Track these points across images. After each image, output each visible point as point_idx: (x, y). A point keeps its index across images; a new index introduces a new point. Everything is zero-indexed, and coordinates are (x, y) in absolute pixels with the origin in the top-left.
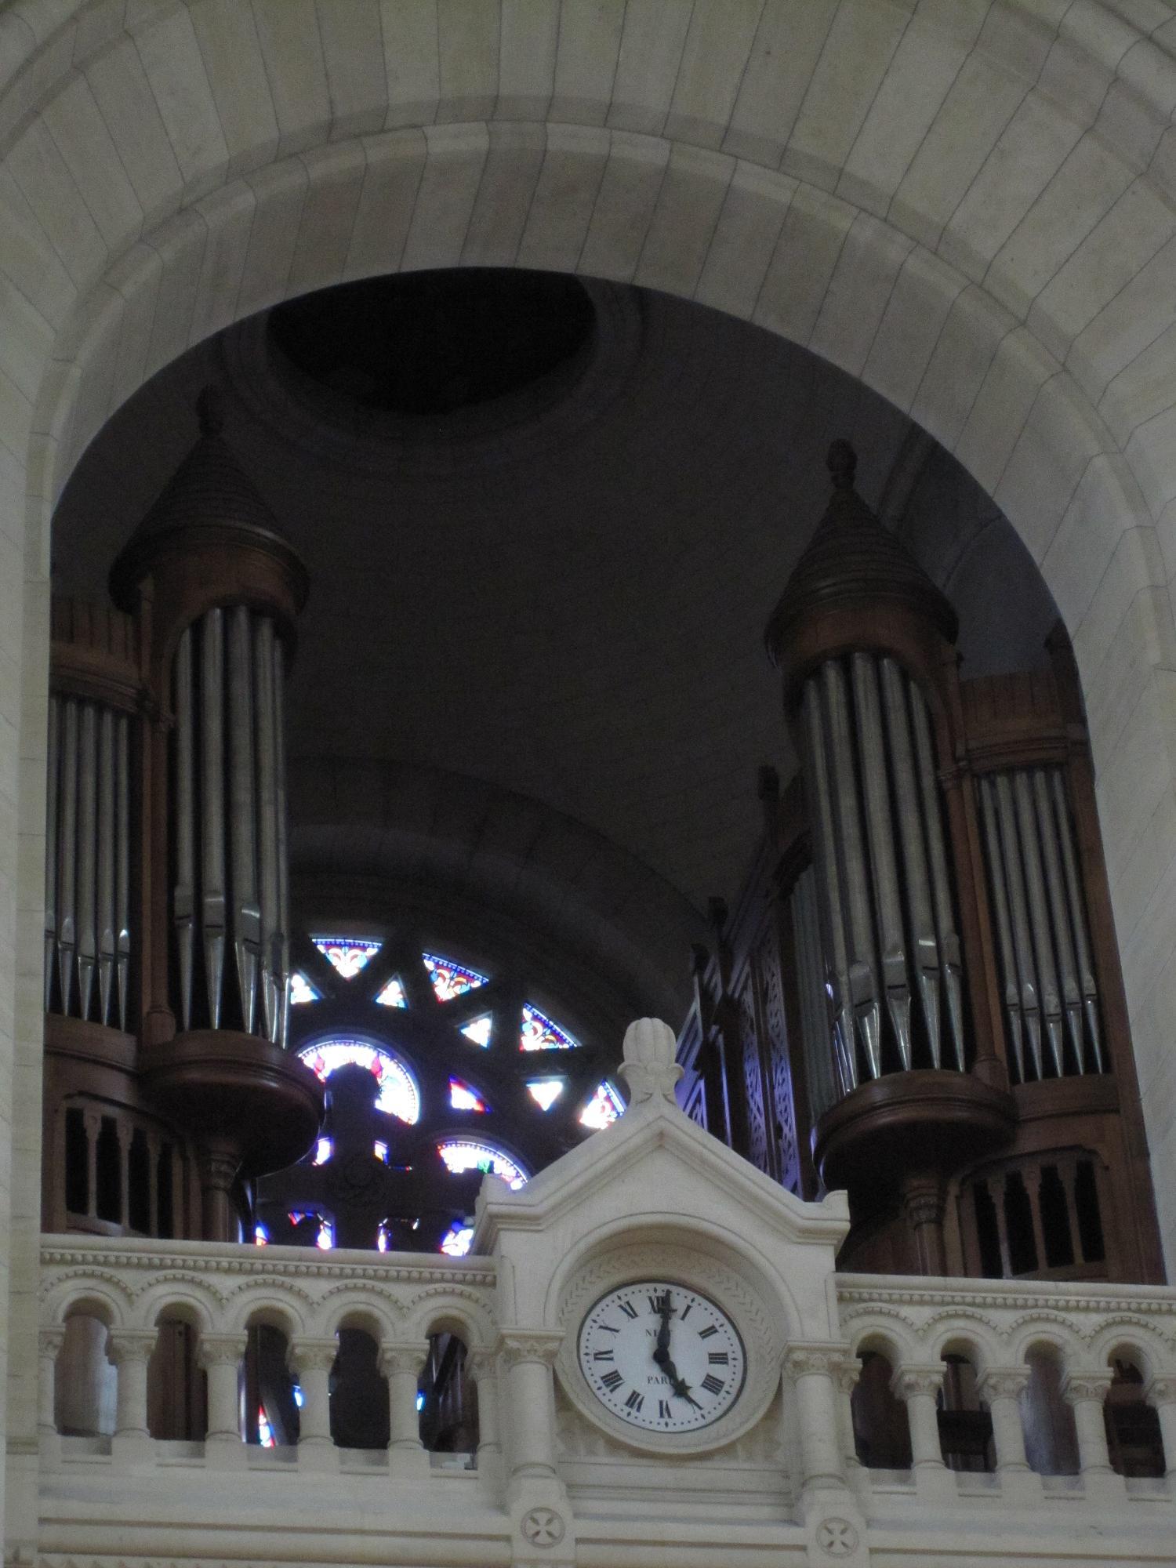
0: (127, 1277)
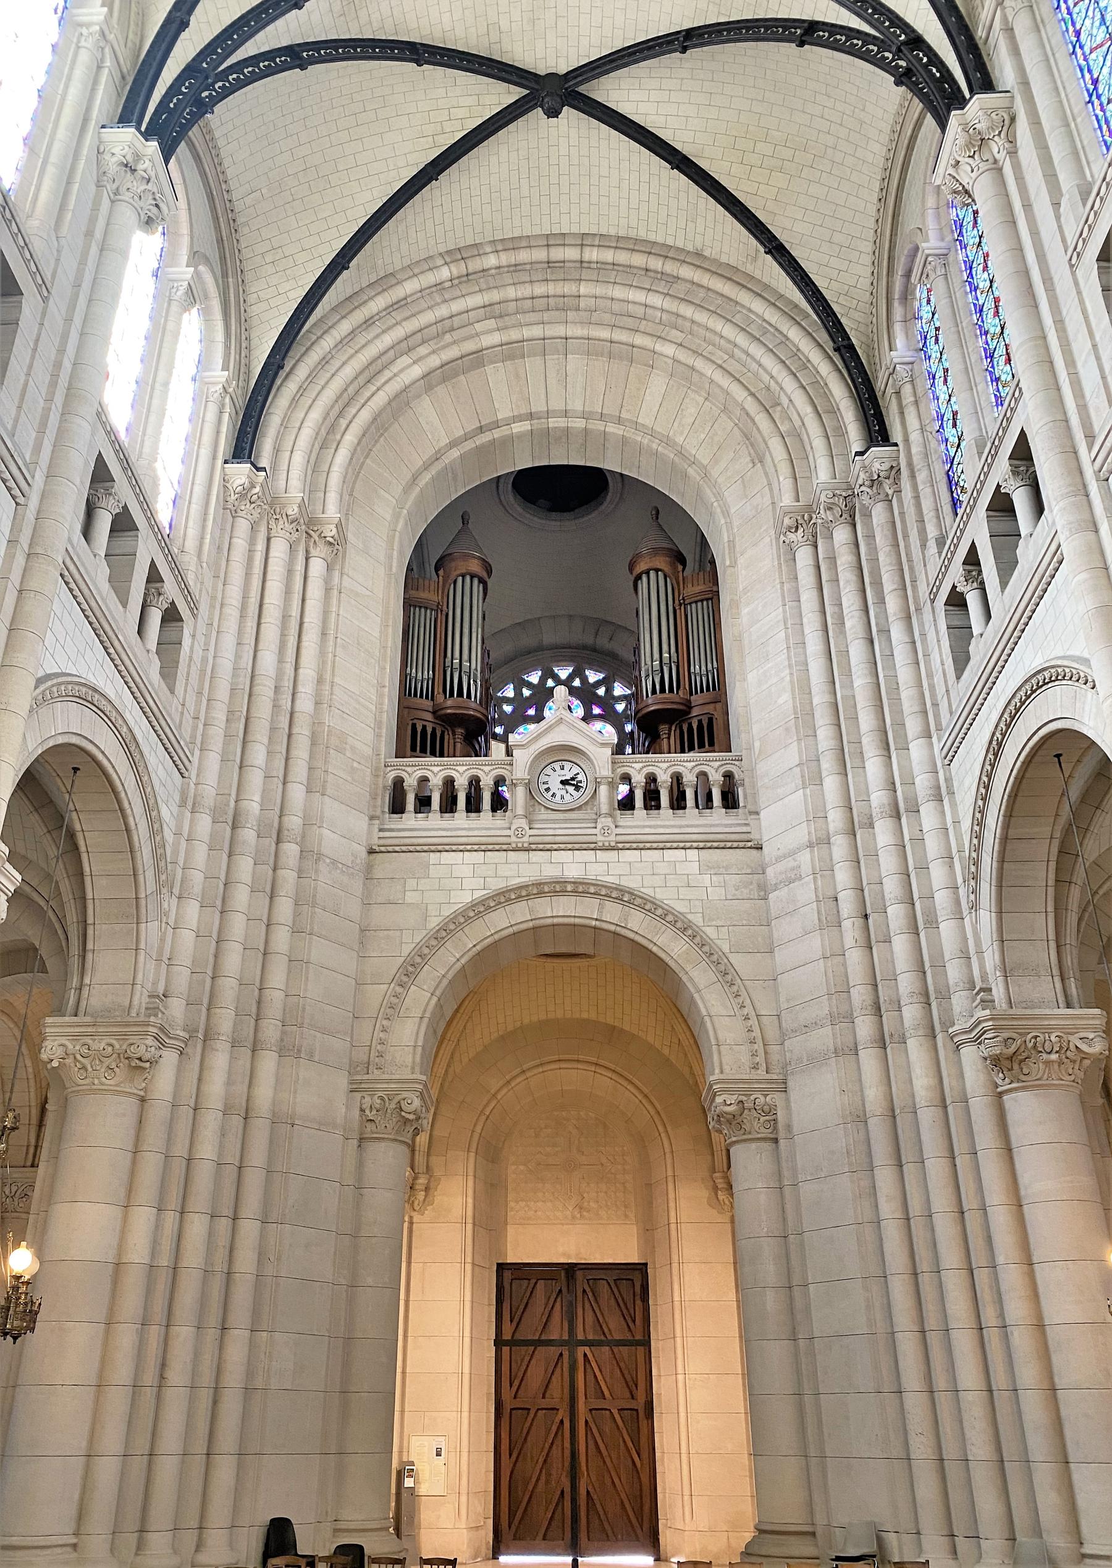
0: (409, 769)
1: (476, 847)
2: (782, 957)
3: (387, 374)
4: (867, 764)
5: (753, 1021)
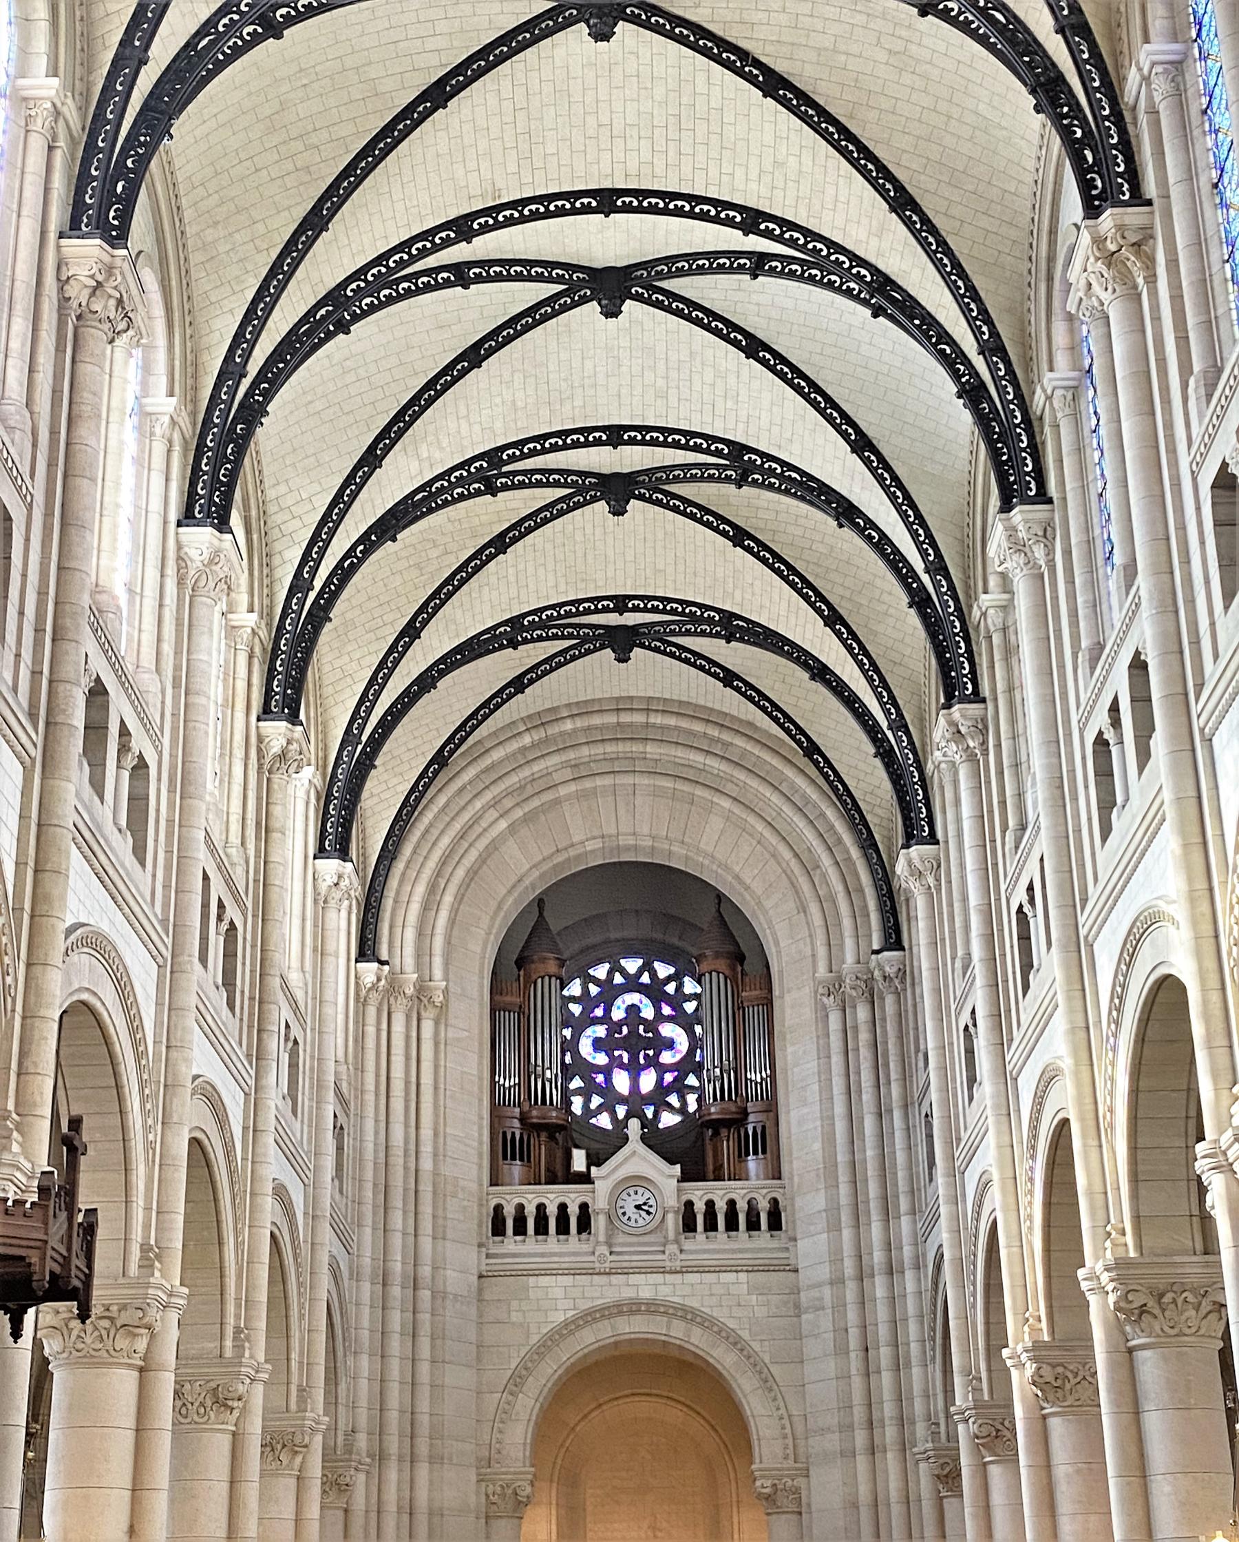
0: (507, 1197)
2: (808, 1368)
3: (478, 829)
4: (873, 1225)
5: (786, 1422)
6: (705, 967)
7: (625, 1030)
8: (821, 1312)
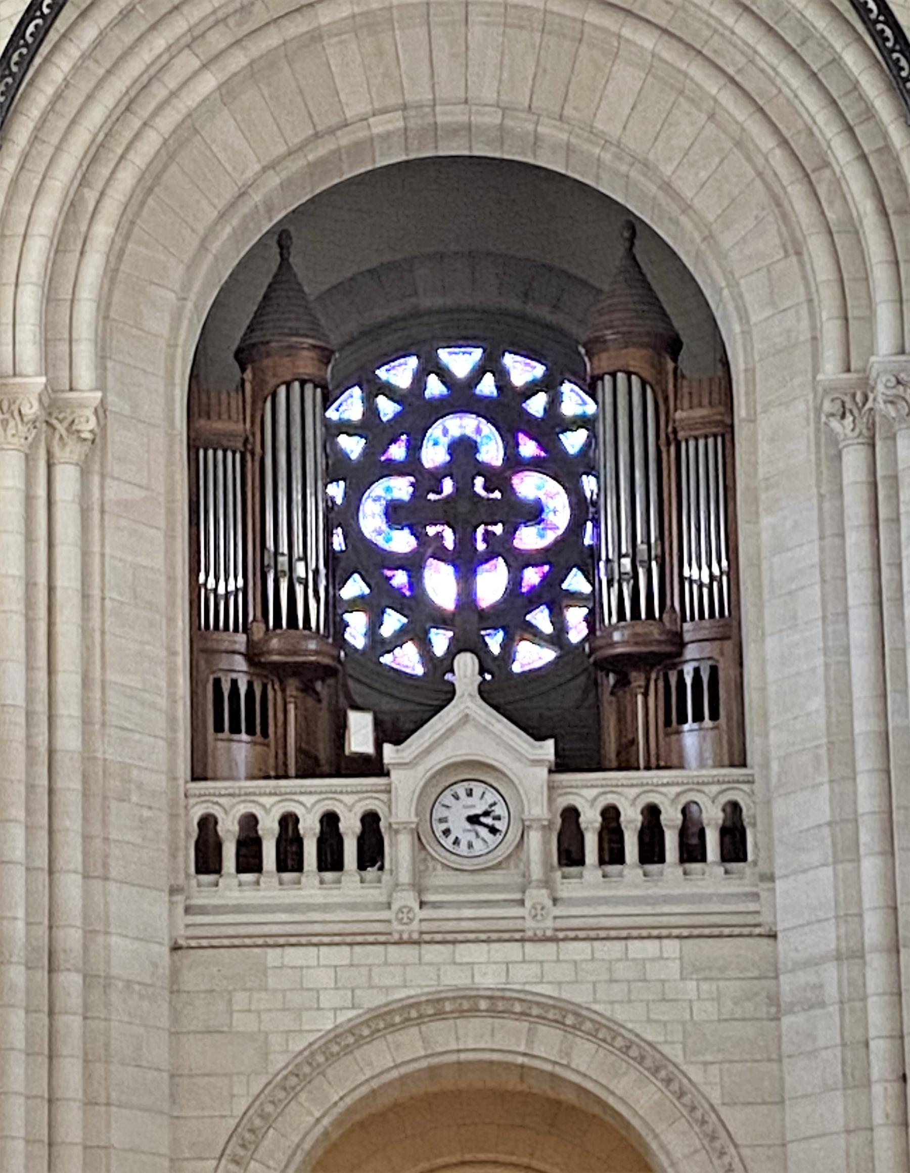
1: (337, 939)
3: (159, 92)
6: (604, 362)
7: (448, 486)
8: (818, 1012)
